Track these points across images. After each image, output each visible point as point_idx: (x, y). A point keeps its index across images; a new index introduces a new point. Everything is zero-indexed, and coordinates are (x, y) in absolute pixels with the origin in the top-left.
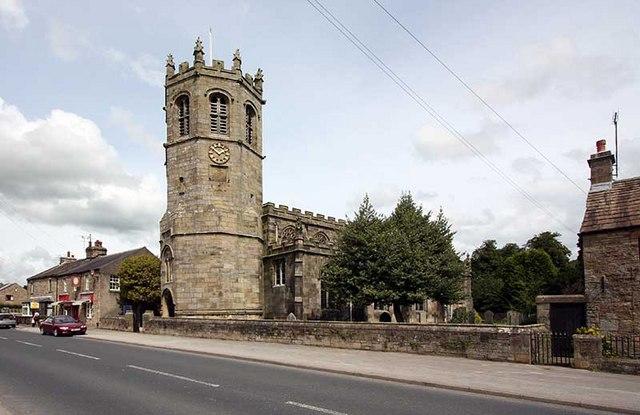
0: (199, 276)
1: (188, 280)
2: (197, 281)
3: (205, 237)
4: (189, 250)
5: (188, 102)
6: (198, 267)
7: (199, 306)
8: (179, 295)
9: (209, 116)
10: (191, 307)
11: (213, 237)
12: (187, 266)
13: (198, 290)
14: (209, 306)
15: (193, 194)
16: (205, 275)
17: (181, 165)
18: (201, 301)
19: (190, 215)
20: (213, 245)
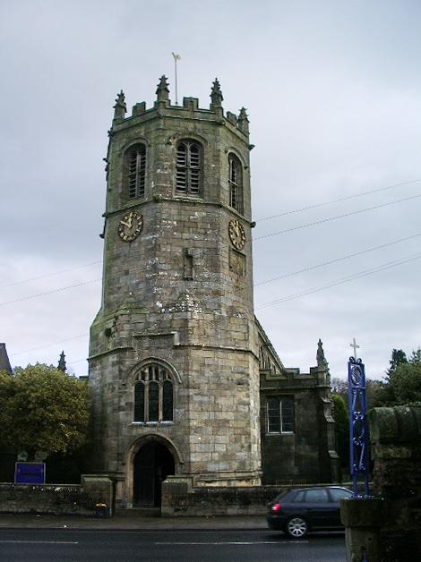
0: (222, 416)
1: (206, 422)
2: (220, 425)
3: (231, 356)
4: (208, 373)
5: (143, 153)
6: (222, 401)
7: (222, 466)
8: (193, 448)
9: (175, 171)
10: (211, 467)
11: (241, 356)
12: (206, 399)
13: (221, 439)
14: (235, 465)
15: (213, 286)
16: (230, 416)
17: (186, 235)
18: (226, 457)
19: (210, 317)
20: (241, 370)
